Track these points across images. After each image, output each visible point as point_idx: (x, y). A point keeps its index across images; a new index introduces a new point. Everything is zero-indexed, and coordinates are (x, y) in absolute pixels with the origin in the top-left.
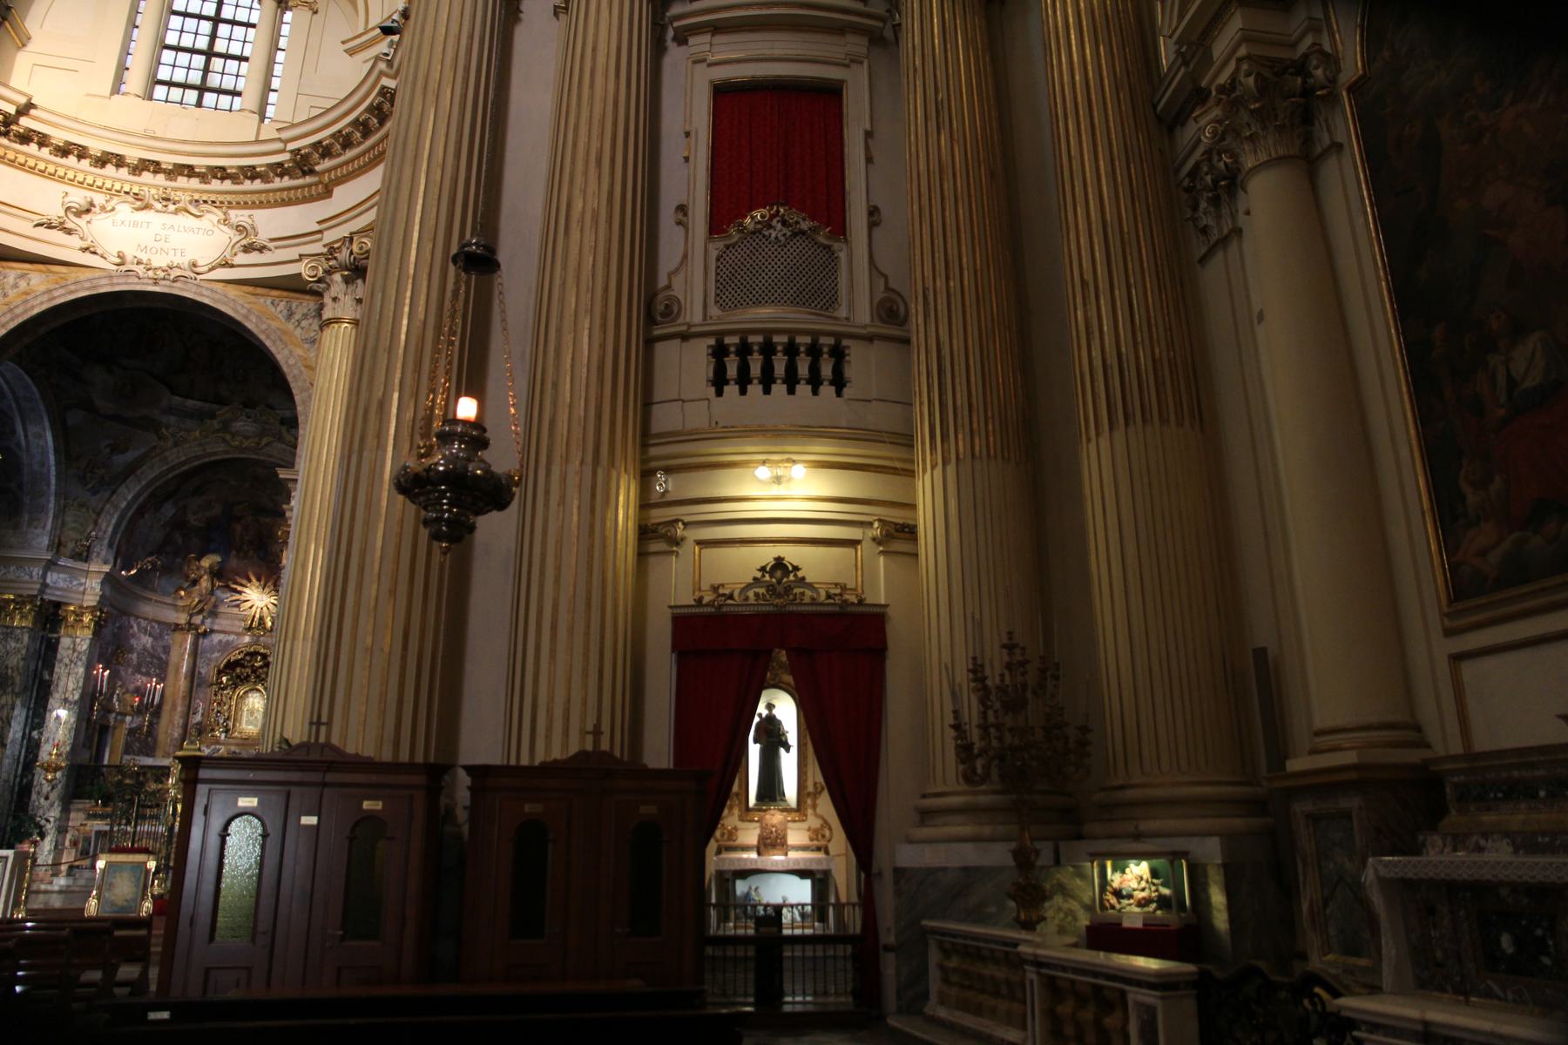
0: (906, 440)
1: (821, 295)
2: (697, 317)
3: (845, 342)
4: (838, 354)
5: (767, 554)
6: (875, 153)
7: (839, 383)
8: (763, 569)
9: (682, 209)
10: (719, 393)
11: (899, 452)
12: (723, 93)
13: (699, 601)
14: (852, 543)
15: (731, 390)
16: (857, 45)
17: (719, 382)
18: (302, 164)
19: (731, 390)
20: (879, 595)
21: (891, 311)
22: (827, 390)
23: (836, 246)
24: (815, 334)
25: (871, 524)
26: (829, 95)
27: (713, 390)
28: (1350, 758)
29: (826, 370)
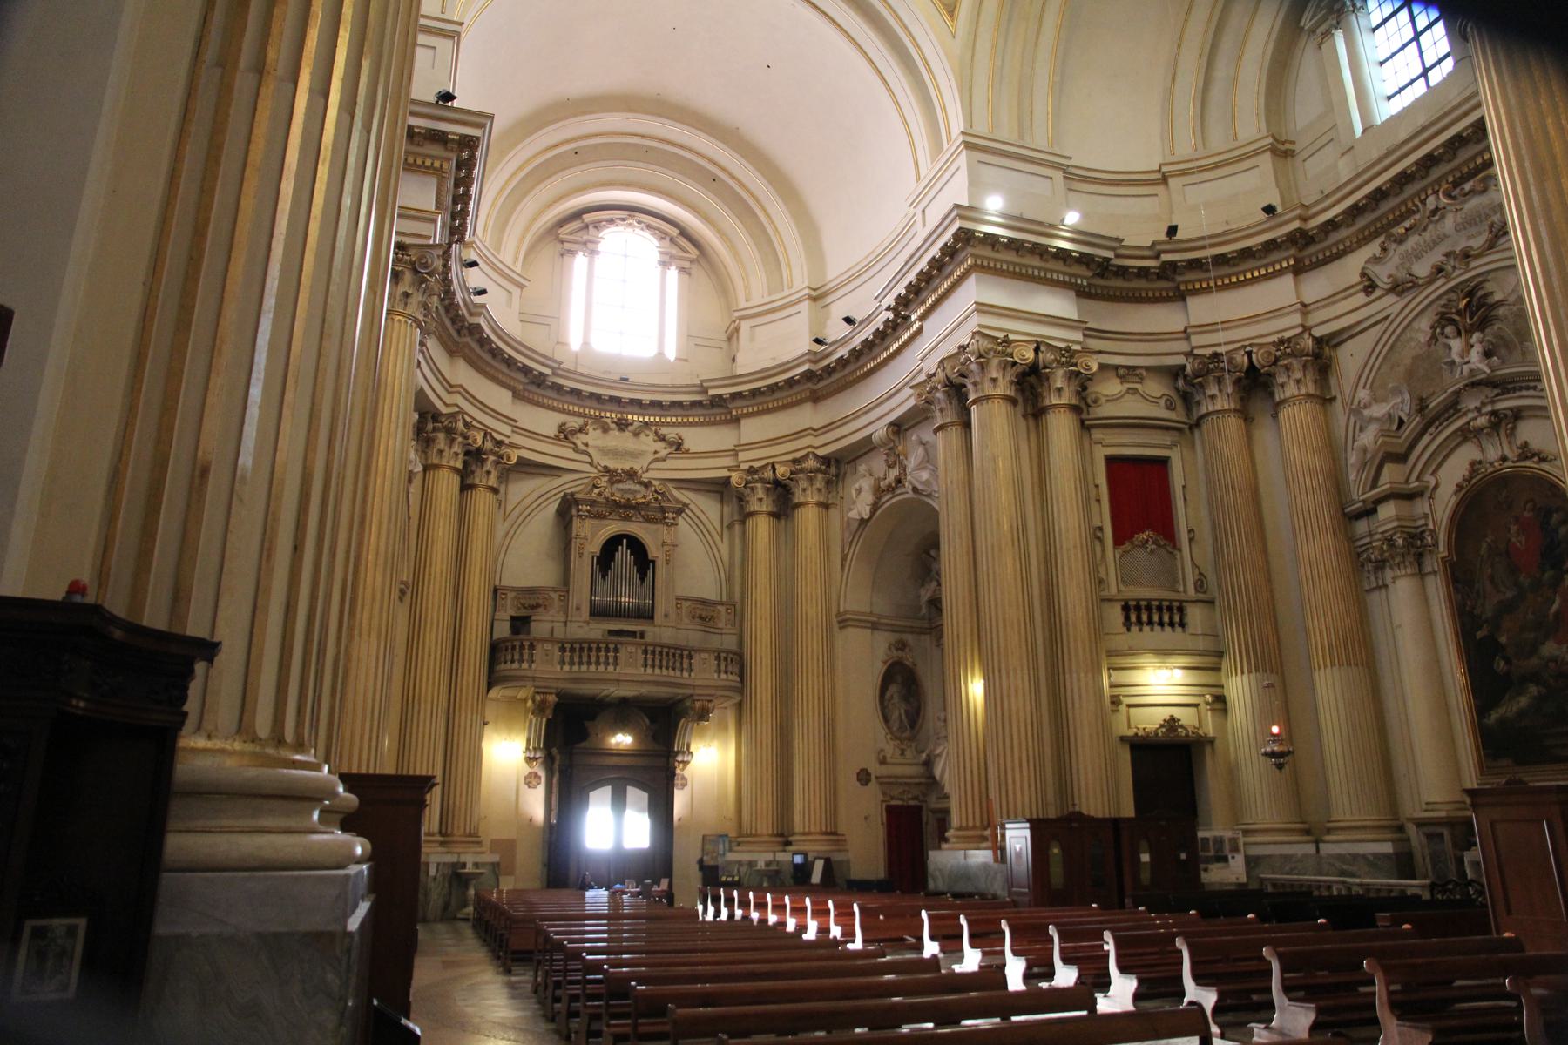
0: (1220, 655)
1: (1172, 581)
2: (1114, 590)
3: (1184, 604)
4: (1181, 610)
5: (1165, 713)
6: (1188, 498)
7: (1182, 625)
8: (1165, 721)
9: (1101, 529)
10: (1129, 630)
11: (1215, 659)
12: (1111, 461)
13: (1136, 734)
14: (1196, 705)
15: (1134, 629)
16: (1174, 436)
17: (1127, 623)
18: (717, 402)
19: (1134, 629)
20: (1209, 729)
21: (1200, 584)
22: (1179, 629)
23: (1176, 552)
24: (1171, 601)
25: (1203, 695)
26: (1163, 462)
27: (1125, 629)
28: (1443, 814)
29: (1177, 618)
